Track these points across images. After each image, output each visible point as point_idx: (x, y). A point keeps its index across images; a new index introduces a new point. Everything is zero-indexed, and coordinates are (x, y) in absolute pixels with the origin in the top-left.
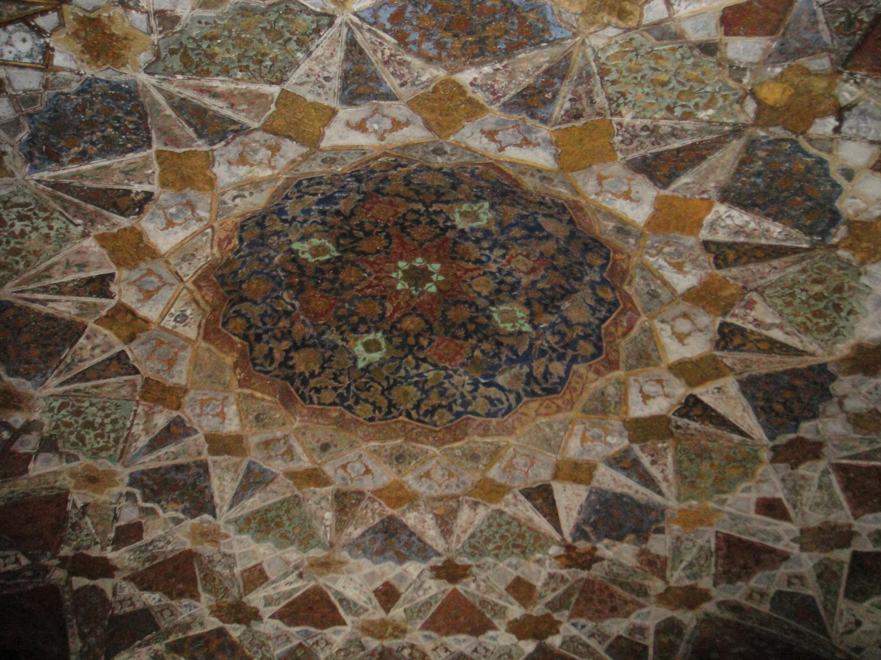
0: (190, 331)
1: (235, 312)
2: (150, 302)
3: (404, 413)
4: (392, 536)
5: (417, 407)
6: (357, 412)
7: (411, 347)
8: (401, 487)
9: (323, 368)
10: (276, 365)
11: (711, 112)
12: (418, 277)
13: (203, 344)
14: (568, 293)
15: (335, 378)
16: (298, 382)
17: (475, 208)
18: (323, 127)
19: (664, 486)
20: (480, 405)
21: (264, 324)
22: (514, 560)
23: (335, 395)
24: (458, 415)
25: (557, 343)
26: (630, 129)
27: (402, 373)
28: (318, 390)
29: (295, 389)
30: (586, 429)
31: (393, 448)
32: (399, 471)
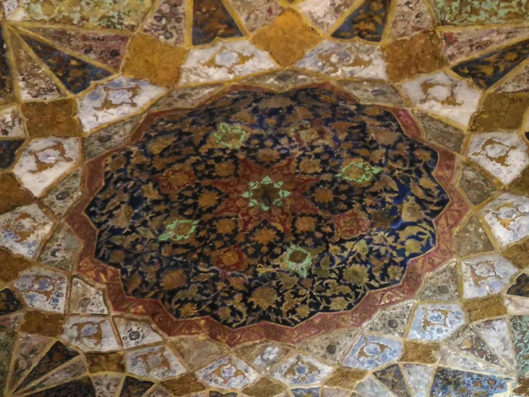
0: (153, 337)
1: (176, 303)
2: (104, 340)
3: (367, 288)
4: (457, 384)
5: (372, 277)
6: (335, 309)
7: (324, 238)
8: (416, 345)
9: (279, 295)
10: (245, 315)
12: (266, 194)
13: (173, 339)
16: (273, 317)
17: (224, 131)
18: (19, 185)
20: (411, 246)
21: (207, 295)
23: (307, 307)
24: (403, 264)
25: (405, 165)
26: (155, 27)
27: (338, 261)
30: (497, 216)
31: (380, 319)
32: (401, 334)
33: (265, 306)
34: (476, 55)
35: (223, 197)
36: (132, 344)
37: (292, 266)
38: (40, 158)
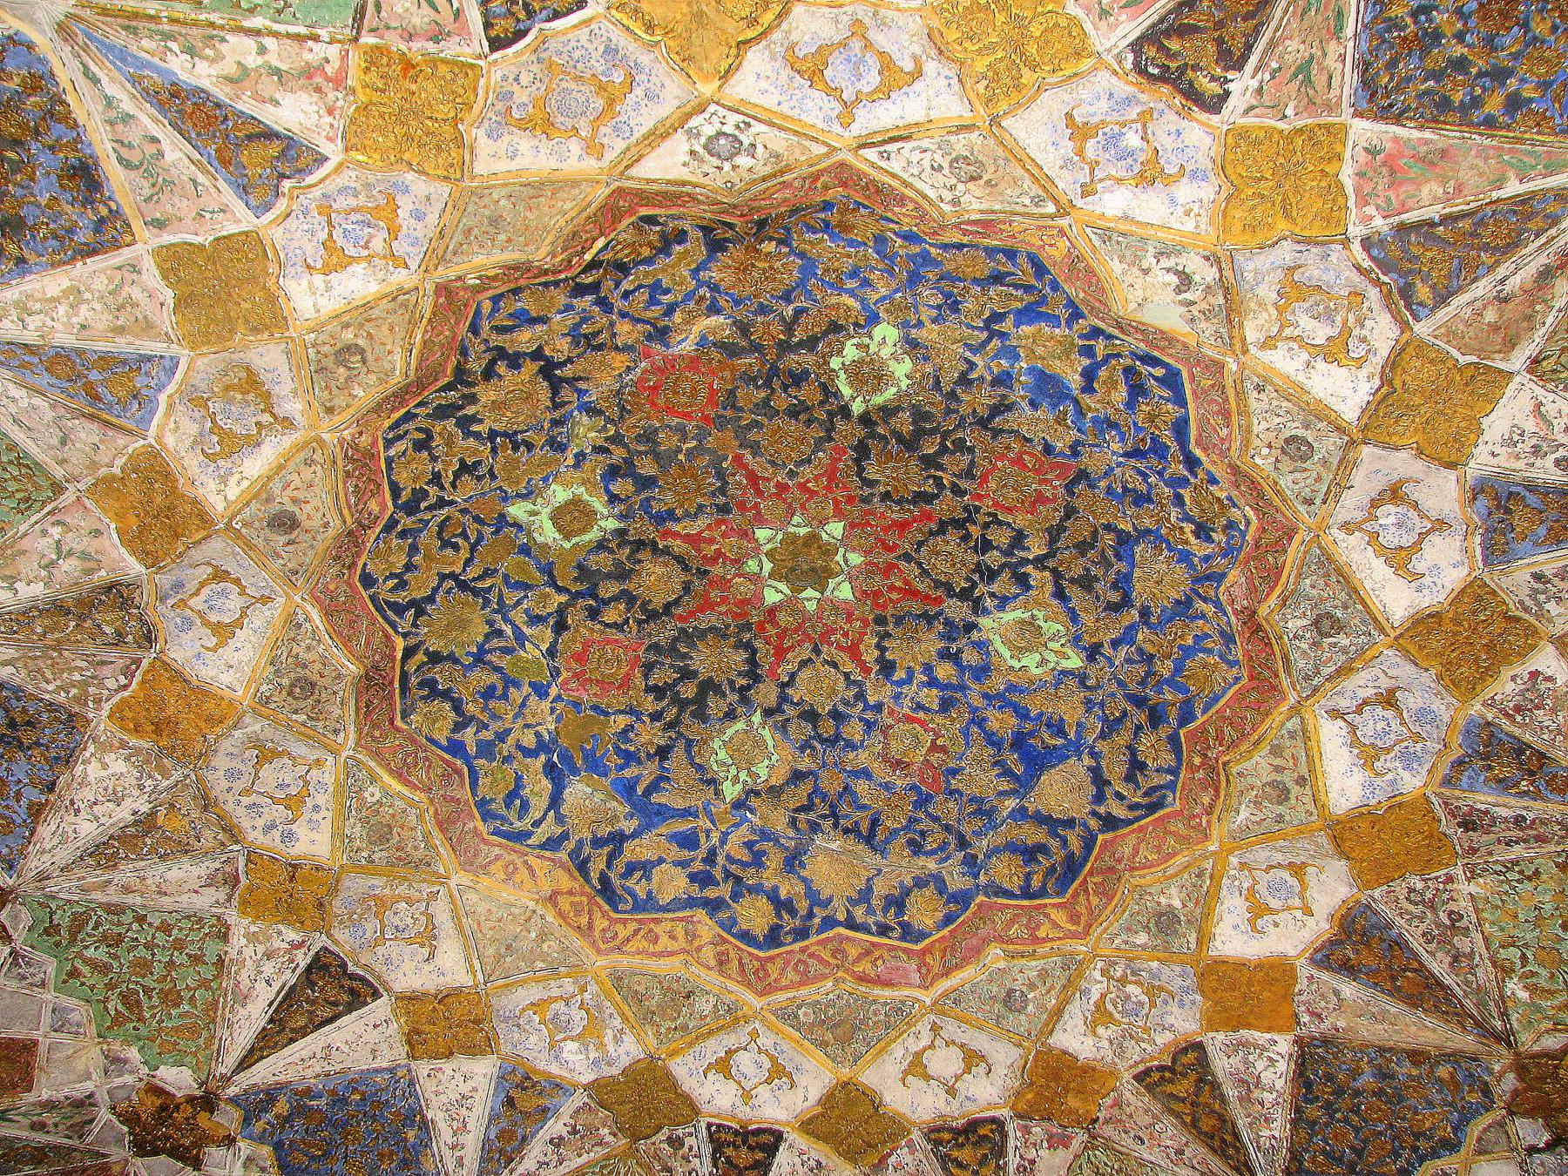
0: (667, 164)
3: (412, 641)
5: (435, 658)
9: (493, 435)
10: (497, 340)
11: (1524, 995)
15: (464, 468)
24: (456, 748)
25: (729, 858)
27: (511, 597)
33: (487, 394)
38: (1412, 513)
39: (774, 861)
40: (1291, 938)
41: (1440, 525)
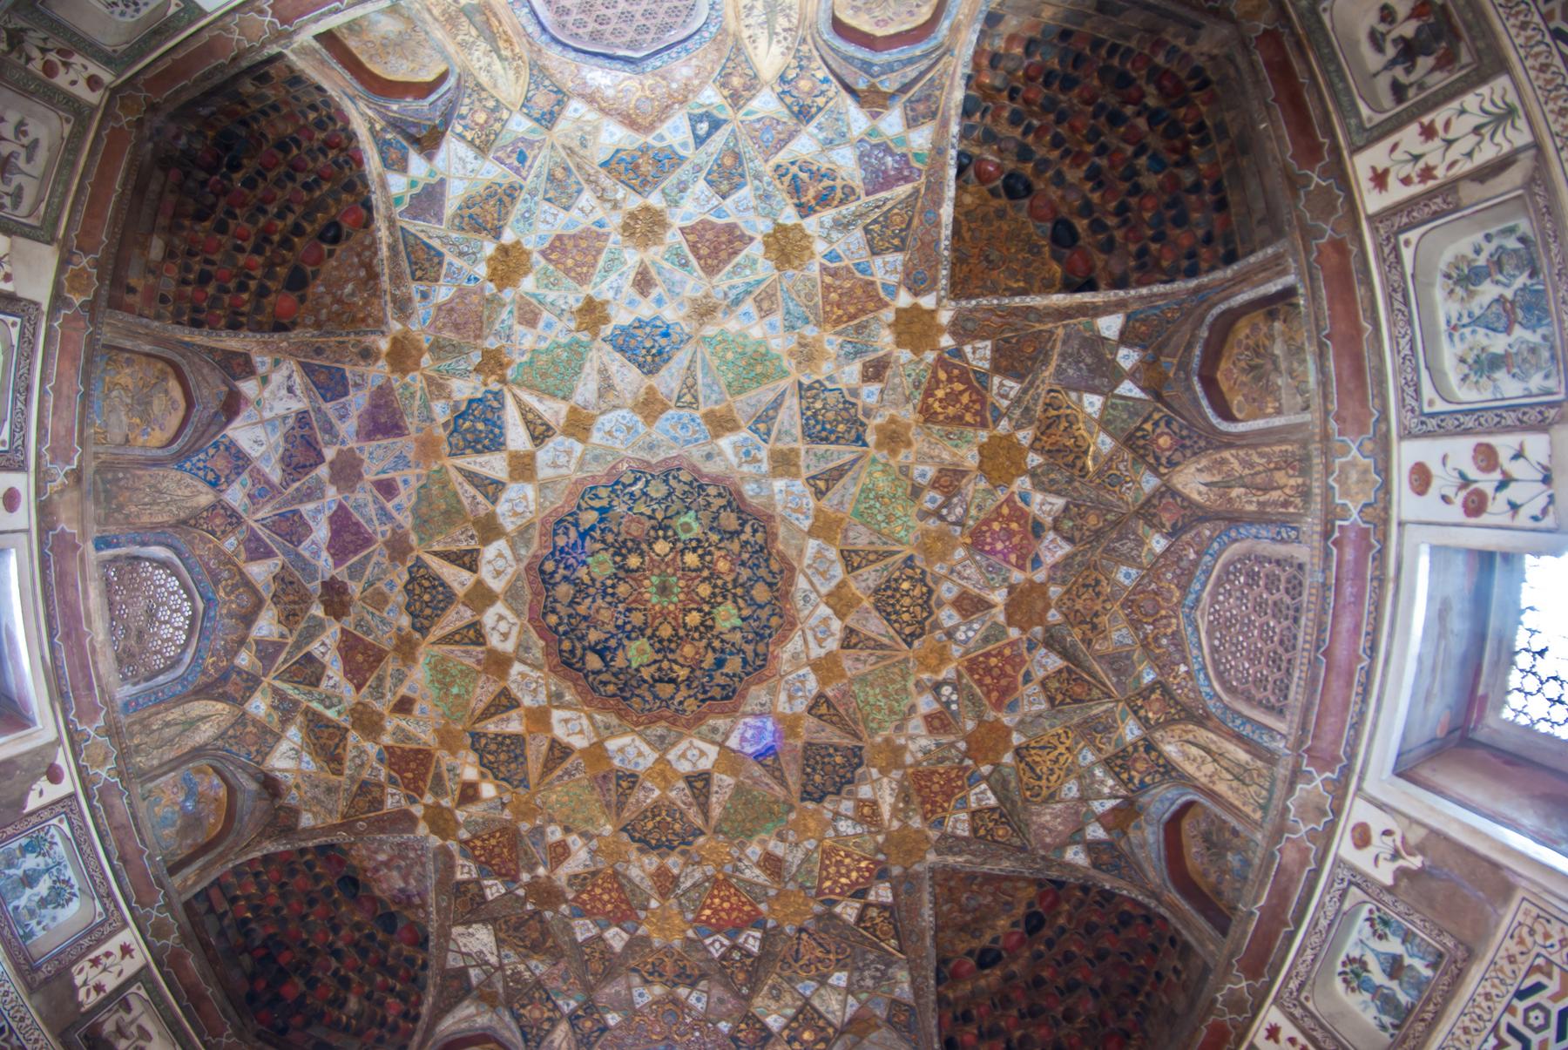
0: (802, 583)
12: (664, 590)
14: (572, 603)
19: (461, 479)
20: (603, 493)
22: (543, 345)
24: (617, 483)
28: (720, 495)
29: (735, 501)
33: (734, 516)
34: (471, 648)
35: (686, 612)
36: (813, 596)
37: (695, 525)
39: (567, 573)
40: (559, 731)
41: (694, 764)
